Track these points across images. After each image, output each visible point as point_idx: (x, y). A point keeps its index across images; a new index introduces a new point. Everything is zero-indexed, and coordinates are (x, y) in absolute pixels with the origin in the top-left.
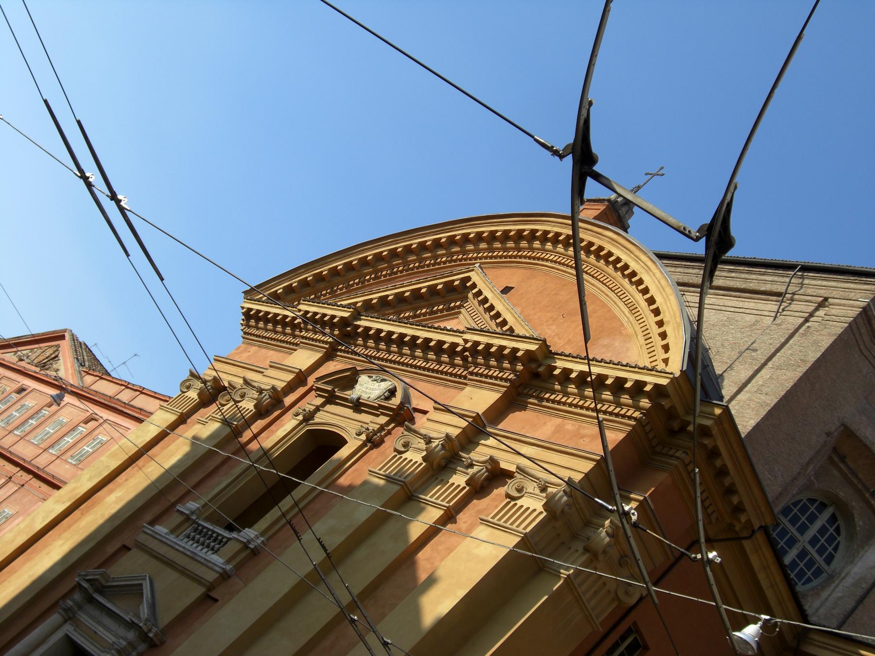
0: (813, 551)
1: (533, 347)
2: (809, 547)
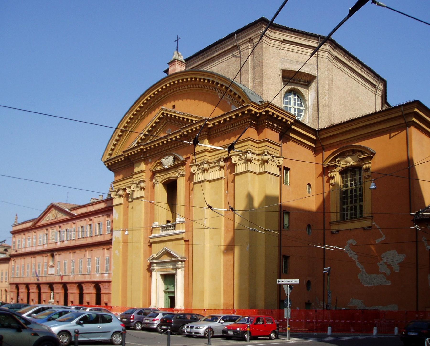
0: (296, 107)
2: (295, 107)
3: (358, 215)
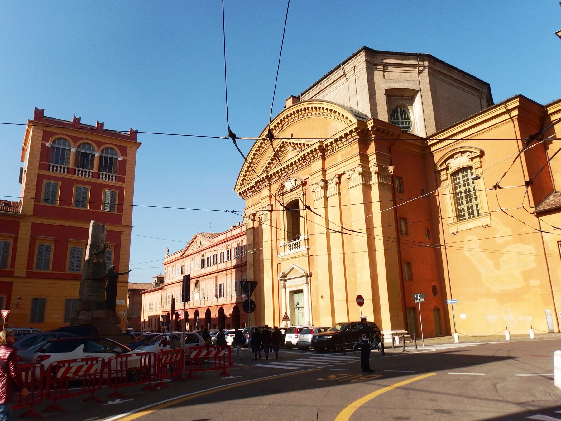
0: (404, 120)
1: (318, 144)
2: (402, 120)
3: (476, 215)
